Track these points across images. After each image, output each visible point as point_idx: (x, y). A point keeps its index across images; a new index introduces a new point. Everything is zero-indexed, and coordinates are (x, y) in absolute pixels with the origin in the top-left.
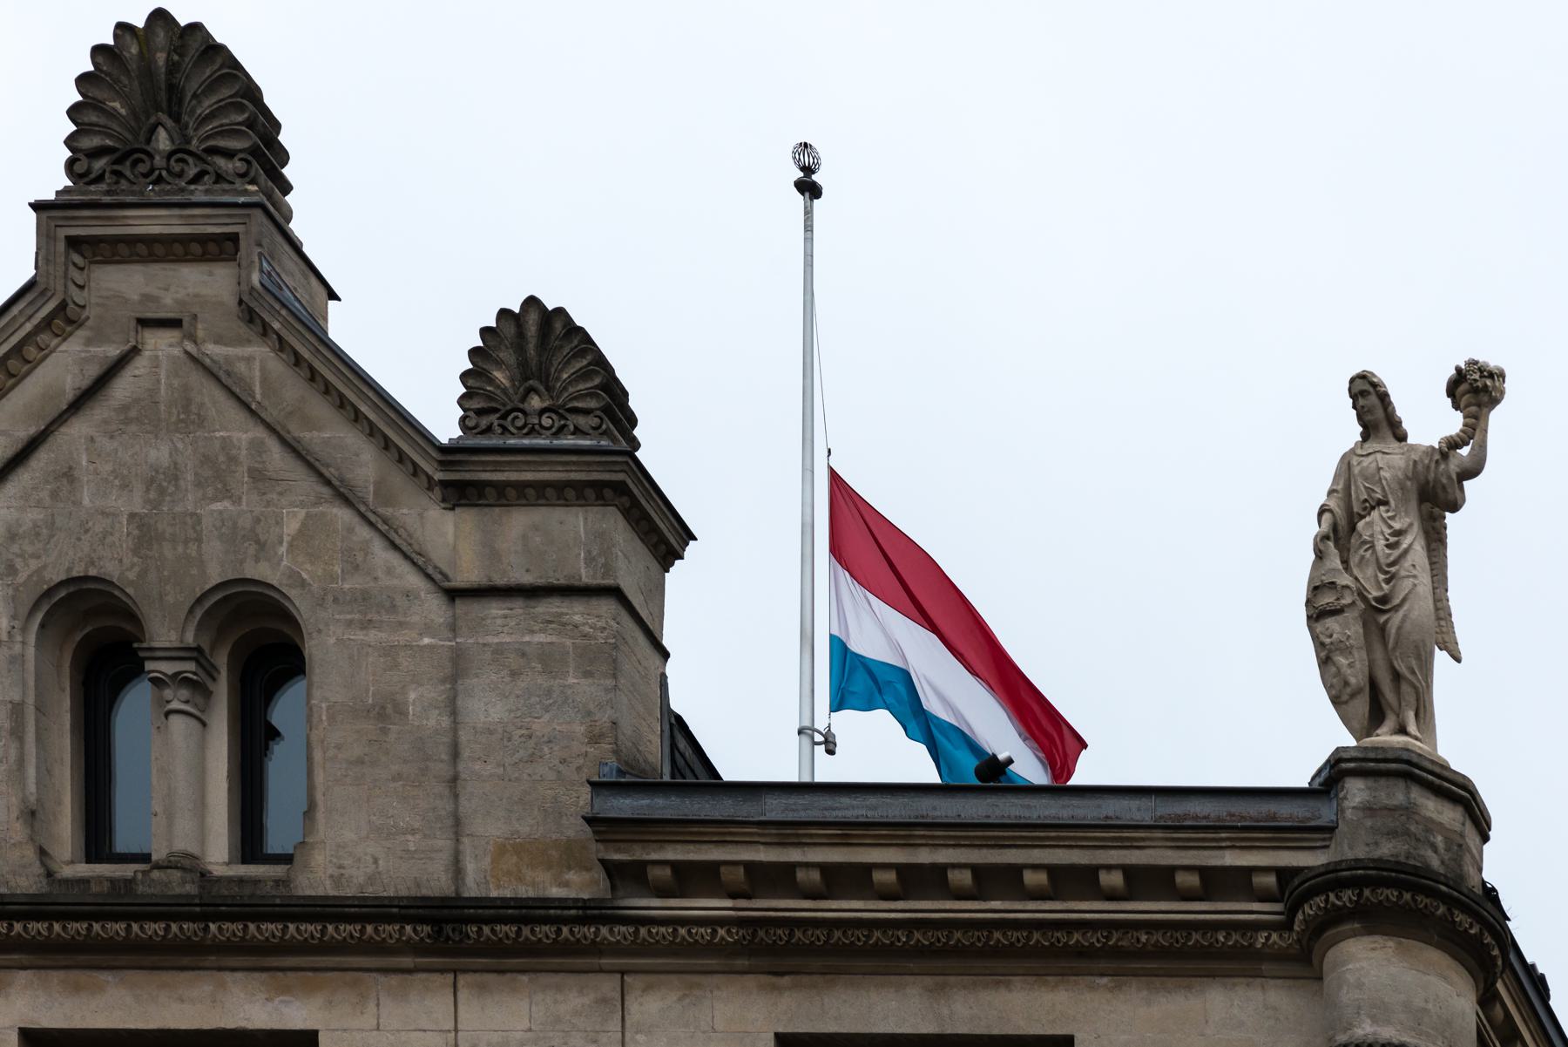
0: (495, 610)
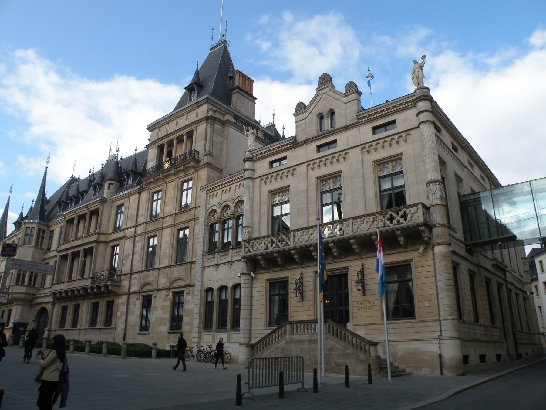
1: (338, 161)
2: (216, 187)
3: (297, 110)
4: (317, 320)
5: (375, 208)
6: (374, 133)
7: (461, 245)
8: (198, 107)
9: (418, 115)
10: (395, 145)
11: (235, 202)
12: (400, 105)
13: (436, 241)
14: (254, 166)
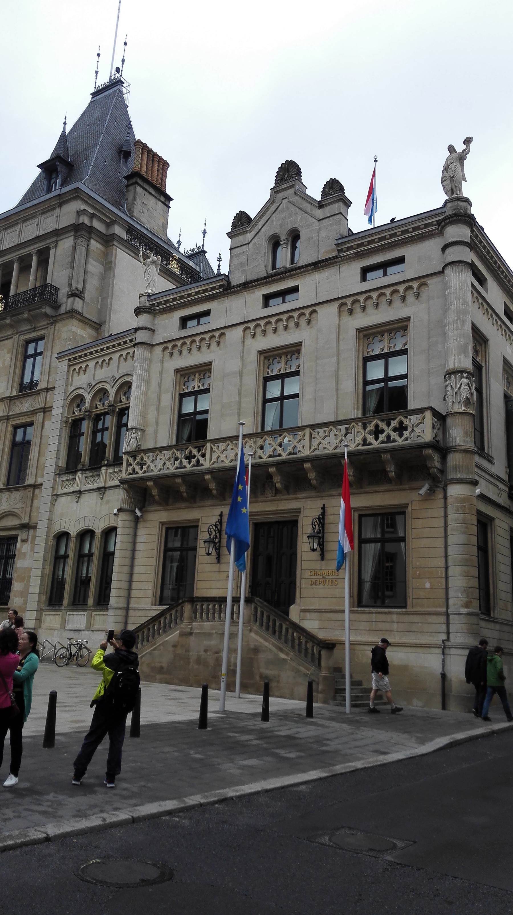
0: (324, 221)
1: (297, 325)
2: (86, 355)
3: (234, 225)
4: (240, 598)
5: (353, 411)
6: (364, 279)
7: (501, 486)
8: (61, 205)
9: (444, 249)
10: (397, 302)
11: (117, 383)
12: (415, 229)
13: (451, 475)
14: (153, 324)
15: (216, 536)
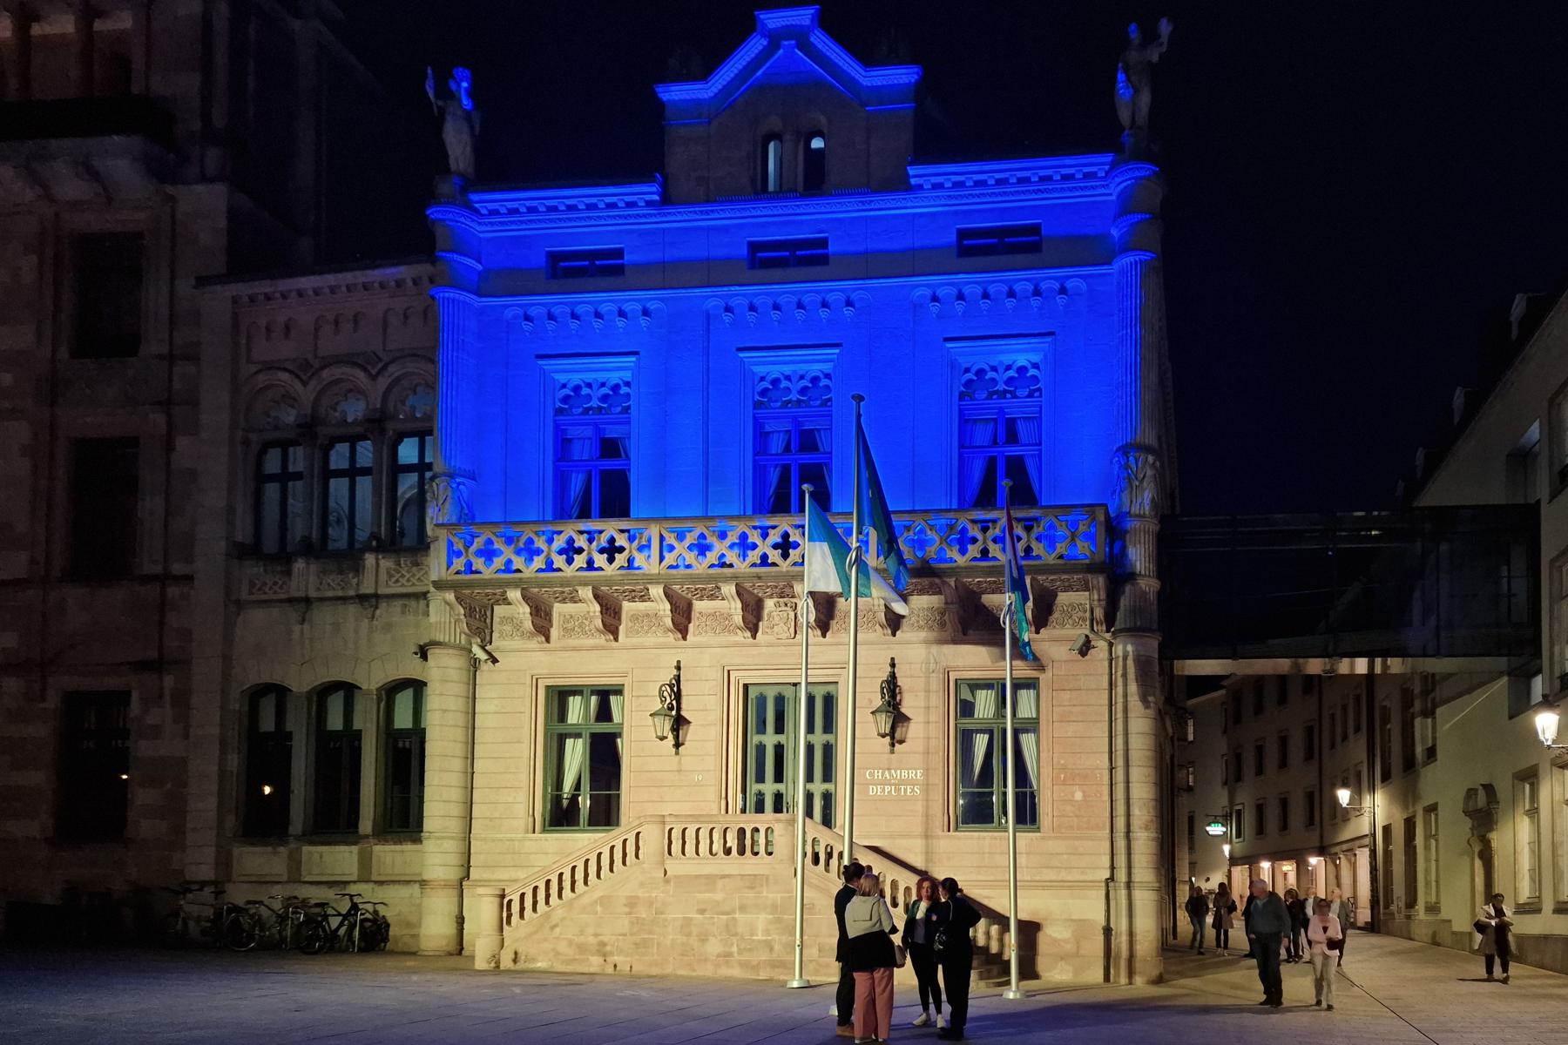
15: (672, 705)
